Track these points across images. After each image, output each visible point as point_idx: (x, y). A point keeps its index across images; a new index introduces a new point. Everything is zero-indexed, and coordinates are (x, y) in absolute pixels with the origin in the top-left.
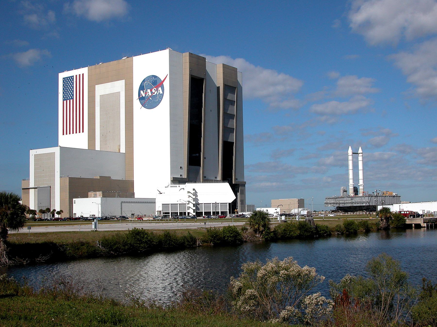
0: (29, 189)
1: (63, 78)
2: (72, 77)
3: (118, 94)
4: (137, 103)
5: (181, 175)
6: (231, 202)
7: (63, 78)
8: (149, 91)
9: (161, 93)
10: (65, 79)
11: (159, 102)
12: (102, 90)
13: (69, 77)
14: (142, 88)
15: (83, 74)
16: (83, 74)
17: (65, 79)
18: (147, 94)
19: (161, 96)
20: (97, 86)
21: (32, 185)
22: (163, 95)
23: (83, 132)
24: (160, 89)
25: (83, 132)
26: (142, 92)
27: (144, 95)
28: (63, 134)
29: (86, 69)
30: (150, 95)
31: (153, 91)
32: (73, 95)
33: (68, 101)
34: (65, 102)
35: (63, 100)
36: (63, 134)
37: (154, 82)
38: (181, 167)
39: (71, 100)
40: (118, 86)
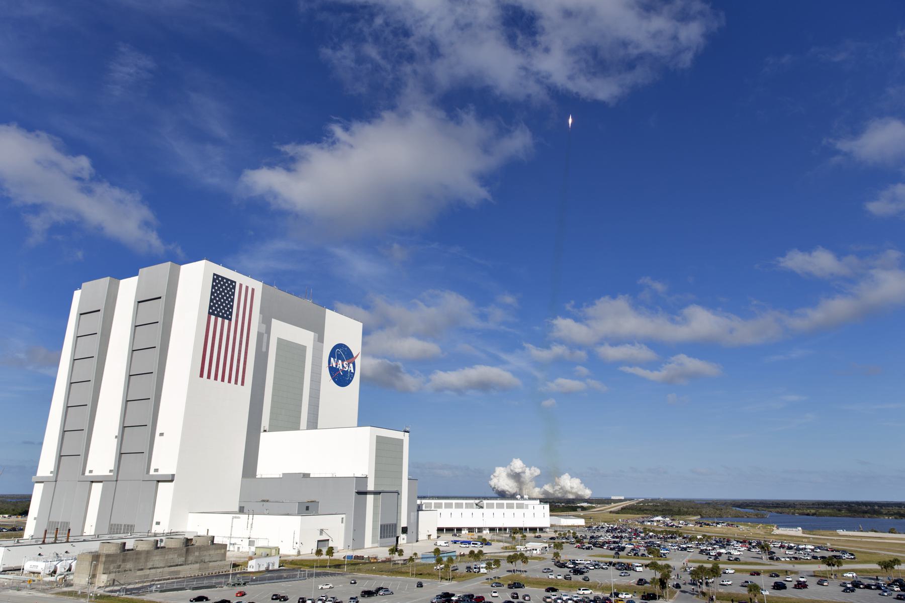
0: (366, 493)
1: (214, 274)
2: (232, 282)
3: (303, 348)
7: (214, 274)
8: (340, 361)
11: (350, 381)
13: (228, 280)
14: (332, 354)
15: (253, 290)
16: (253, 290)
20: (273, 320)
23: (243, 384)
24: (351, 365)
25: (243, 384)
28: (201, 375)
32: (231, 314)
36: (201, 375)
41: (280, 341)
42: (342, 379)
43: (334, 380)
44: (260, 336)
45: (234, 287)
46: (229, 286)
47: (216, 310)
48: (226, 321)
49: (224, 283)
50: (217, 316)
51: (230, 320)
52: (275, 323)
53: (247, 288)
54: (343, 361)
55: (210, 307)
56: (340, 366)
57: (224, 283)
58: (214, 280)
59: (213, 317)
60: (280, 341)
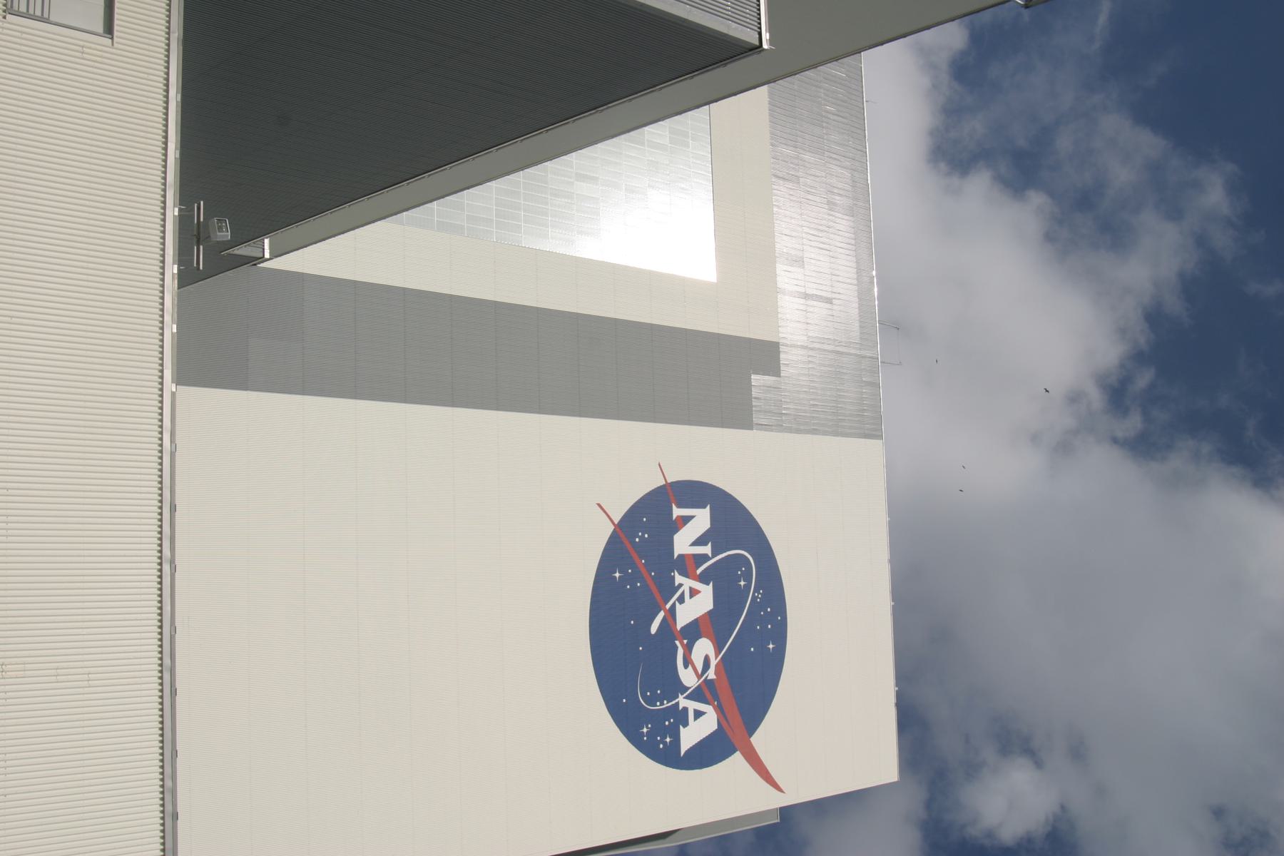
11: (629, 718)
27: (683, 543)
31: (704, 647)
43: (614, 554)
56: (696, 603)
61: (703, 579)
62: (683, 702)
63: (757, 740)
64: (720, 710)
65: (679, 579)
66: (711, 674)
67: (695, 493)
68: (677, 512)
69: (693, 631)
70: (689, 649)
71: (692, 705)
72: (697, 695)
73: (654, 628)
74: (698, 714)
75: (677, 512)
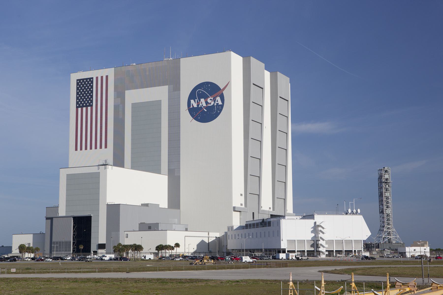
1: (77, 80)
2: (90, 79)
3: (158, 103)
4: (185, 115)
5: (241, 205)
6: (365, 239)
7: (77, 80)
8: (203, 100)
9: (220, 103)
10: (80, 82)
11: (217, 115)
12: (133, 96)
13: (86, 79)
14: (192, 96)
15: (107, 77)
16: (107, 77)
17: (80, 82)
18: (201, 104)
19: (220, 108)
20: (126, 91)
21: (62, 212)
22: (222, 106)
23: (106, 147)
24: (218, 99)
25: (106, 147)
26: (192, 101)
27: (195, 106)
28: (76, 149)
29: (113, 69)
30: (204, 105)
31: (209, 101)
32: (92, 101)
33: (84, 109)
34: (80, 109)
35: (77, 108)
36: (76, 149)
37: (208, 89)
38: (241, 195)
39: (89, 108)
40: (160, 93)
41: (134, 106)
42: (205, 115)
44: (116, 108)
45: (92, 82)
46: (88, 82)
47: (81, 103)
48: (89, 108)
49: (85, 83)
50: (82, 107)
51: (92, 106)
52: (127, 93)
53: (102, 77)
54: (206, 98)
55: (77, 103)
57: (85, 83)
58: (78, 84)
59: (80, 109)
60: (134, 106)
61: (200, 101)
62: (215, 104)
63: (222, 88)
64: (217, 96)
65: (200, 106)
66: (212, 98)
67: (189, 103)
68: (191, 107)
69: (207, 103)
70: (209, 103)
71: (216, 102)
72: (215, 102)
73: (206, 110)
74: (217, 101)
75: (191, 107)
